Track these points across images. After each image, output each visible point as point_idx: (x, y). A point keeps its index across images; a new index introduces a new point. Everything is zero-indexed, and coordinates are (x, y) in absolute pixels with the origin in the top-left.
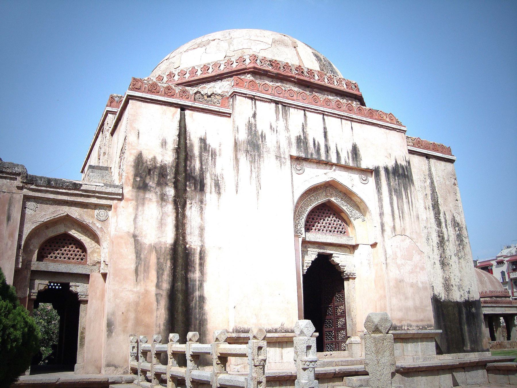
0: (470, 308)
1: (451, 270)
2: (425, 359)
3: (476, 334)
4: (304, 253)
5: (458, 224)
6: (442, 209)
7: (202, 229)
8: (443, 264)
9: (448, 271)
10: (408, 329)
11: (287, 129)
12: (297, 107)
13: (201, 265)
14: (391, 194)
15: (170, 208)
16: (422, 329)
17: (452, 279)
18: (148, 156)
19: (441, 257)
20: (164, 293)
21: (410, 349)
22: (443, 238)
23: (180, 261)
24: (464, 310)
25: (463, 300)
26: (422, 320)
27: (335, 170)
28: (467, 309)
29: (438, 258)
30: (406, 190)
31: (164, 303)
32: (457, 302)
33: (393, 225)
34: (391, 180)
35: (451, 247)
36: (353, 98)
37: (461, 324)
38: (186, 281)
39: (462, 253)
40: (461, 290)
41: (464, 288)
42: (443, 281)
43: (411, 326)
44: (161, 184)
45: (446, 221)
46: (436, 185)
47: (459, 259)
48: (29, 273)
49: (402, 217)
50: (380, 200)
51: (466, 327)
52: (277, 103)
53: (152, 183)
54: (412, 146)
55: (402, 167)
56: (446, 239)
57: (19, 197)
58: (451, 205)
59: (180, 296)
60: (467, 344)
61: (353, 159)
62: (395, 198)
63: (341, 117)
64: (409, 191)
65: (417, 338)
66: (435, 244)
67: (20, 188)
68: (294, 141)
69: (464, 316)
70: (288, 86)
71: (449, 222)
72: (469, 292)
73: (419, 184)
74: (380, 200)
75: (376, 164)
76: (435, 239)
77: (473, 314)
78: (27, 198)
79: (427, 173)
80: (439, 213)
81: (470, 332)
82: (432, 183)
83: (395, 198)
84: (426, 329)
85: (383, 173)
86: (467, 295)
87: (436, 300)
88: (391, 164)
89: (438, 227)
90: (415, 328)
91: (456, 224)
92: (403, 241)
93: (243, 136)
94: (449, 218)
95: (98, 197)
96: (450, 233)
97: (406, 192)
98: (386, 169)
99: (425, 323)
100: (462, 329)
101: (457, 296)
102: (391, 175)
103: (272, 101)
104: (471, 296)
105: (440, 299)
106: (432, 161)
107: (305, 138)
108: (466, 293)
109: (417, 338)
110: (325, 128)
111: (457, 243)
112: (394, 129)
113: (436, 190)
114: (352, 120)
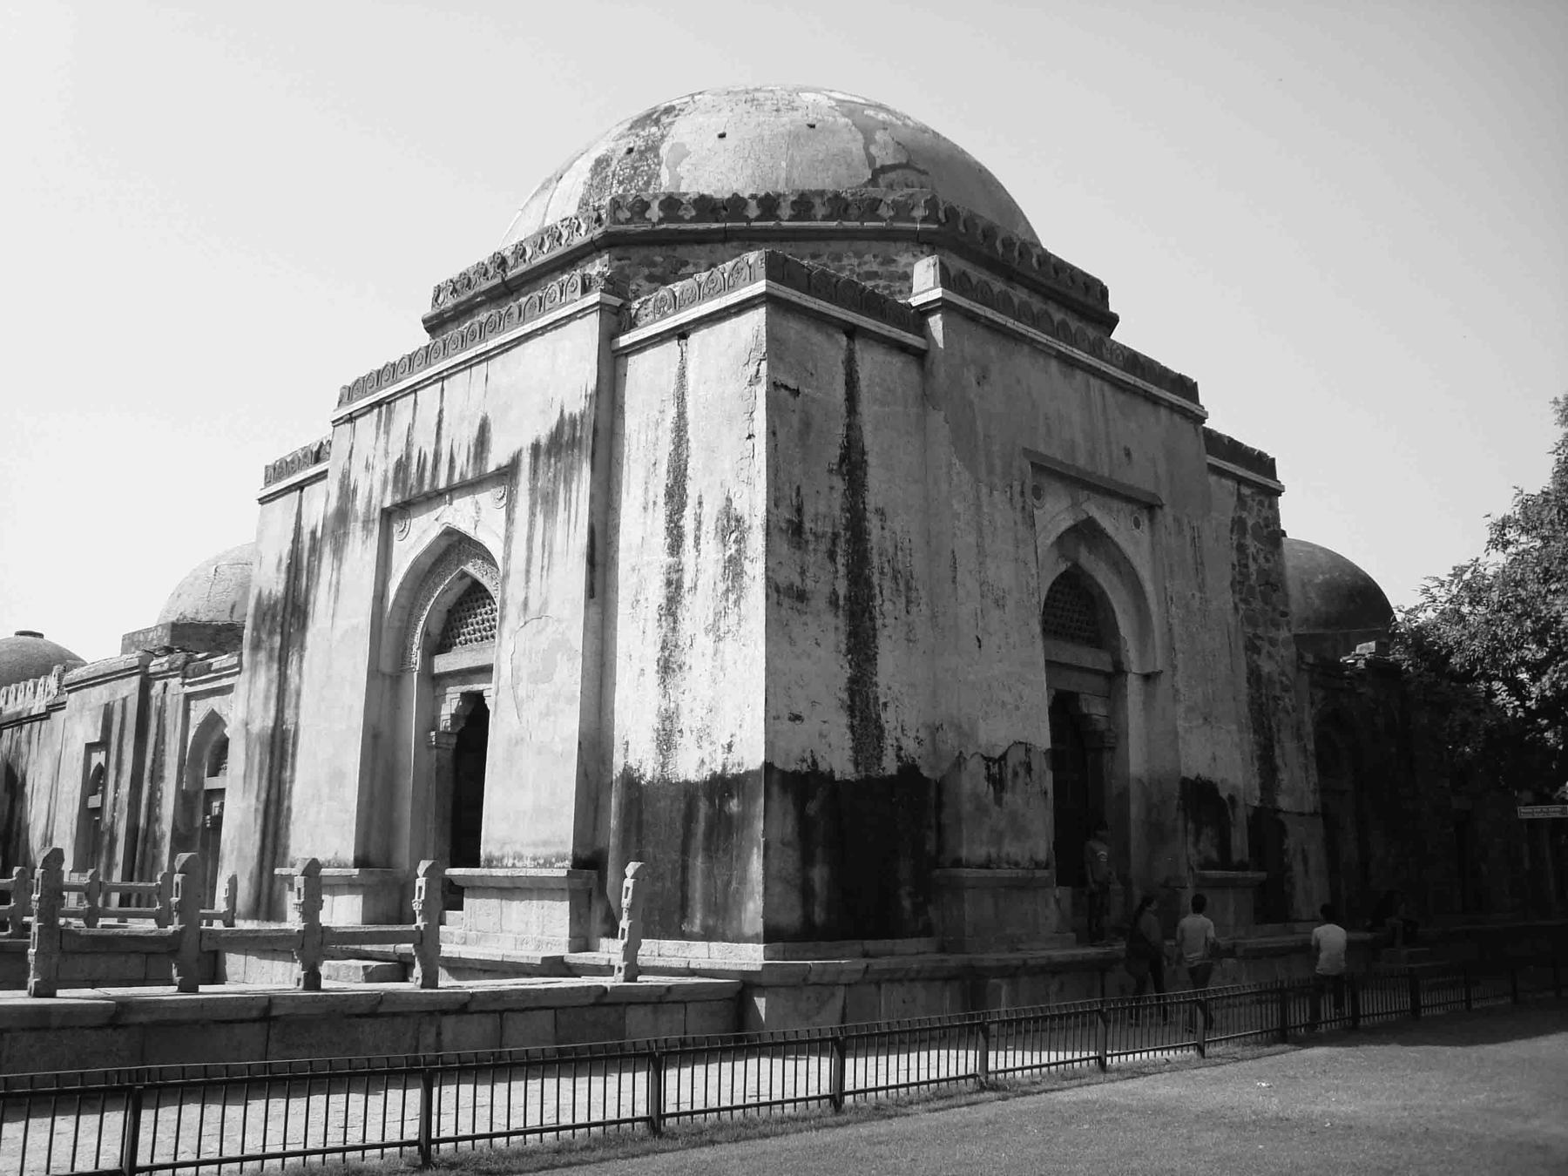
0: (722, 798)
1: (684, 685)
2: (538, 948)
3: (729, 883)
4: (438, 700)
5: (738, 520)
6: (692, 490)
7: (298, 694)
8: (667, 668)
9: (677, 686)
10: (514, 866)
11: (387, 453)
12: (403, 393)
13: (294, 756)
14: (533, 514)
15: (275, 666)
16: (543, 866)
17: (684, 710)
18: (265, 593)
19: (663, 649)
20: (261, 807)
21: (514, 916)
22: (679, 586)
23: (277, 753)
24: (703, 807)
25: (705, 774)
26: (545, 843)
27: (451, 500)
28: (712, 803)
29: (653, 652)
30: (568, 483)
31: (260, 821)
32: (687, 782)
33: (522, 599)
34: (540, 472)
35: (697, 609)
36: (589, 254)
37: (685, 850)
38: (280, 783)
39: (732, 619)
40: (705, 744)
41: (714, 738)
42: (655, 722)
43: (521, 858)
44: (271, 633)
45: (698, 528)
46: (690, 414)
47: (719, 639)
48: (202, 795)
49: (547, 568)
50: (508, 539)
51: (700, 859)
52: (379, 404)
53: (264, 637)
54: (654, 321)
55: (573, 421)
56: (687, 584)
57: (181, 697)
58: (727, 466)
59: (272, 810)
60: (694, 916)
61: (475, 458)
62: (540, 519)
63: (468, 364)
64: (574, 486)
65: (530, 890)
66: (653, 613)
67: (183, 684)
68: (391, 474)
69: (700, 828)
70: (483, 316)
71: (709, 526)
72: (730, 746)
73: (643, 438)
74: (508, 539)
75: (516, 449)
76: (656, 594)
77: (729, 818)
78: (188, 697)
79: (673, 387)
80: (683, 505)
81: (709, 875)
82: (681, 415)
83: (540, 519)
84: (552, 865)
85: (526, 460)
86: (720, 757)
87: (630, 781)
88: (542, 430)
89: (672, 555)
90: (528, 862)
91: (731, 524)
92: (539, 632)
93: (333, 503)
94: (711, 512)
95: (228, 676)
96: (705, 561)
97: (568, 490)
98: (536, 448)
99: (551, 851)
100: (685, 868)
101: (690, 766)
102: (542, 459)
103: (372, 406)
104: (733, 758)
105: (640, 777)
106: (694, 338)
107: (409, 457)
108: (720, 750)
109: (530, 890)
110: (441, 412)
111: (722, 587)
112: (570, 318)
113: (690, 435)
114: (486, 357)
